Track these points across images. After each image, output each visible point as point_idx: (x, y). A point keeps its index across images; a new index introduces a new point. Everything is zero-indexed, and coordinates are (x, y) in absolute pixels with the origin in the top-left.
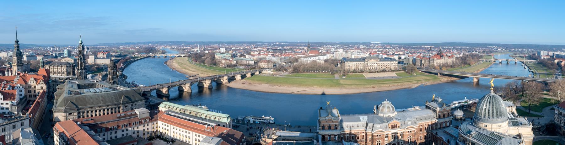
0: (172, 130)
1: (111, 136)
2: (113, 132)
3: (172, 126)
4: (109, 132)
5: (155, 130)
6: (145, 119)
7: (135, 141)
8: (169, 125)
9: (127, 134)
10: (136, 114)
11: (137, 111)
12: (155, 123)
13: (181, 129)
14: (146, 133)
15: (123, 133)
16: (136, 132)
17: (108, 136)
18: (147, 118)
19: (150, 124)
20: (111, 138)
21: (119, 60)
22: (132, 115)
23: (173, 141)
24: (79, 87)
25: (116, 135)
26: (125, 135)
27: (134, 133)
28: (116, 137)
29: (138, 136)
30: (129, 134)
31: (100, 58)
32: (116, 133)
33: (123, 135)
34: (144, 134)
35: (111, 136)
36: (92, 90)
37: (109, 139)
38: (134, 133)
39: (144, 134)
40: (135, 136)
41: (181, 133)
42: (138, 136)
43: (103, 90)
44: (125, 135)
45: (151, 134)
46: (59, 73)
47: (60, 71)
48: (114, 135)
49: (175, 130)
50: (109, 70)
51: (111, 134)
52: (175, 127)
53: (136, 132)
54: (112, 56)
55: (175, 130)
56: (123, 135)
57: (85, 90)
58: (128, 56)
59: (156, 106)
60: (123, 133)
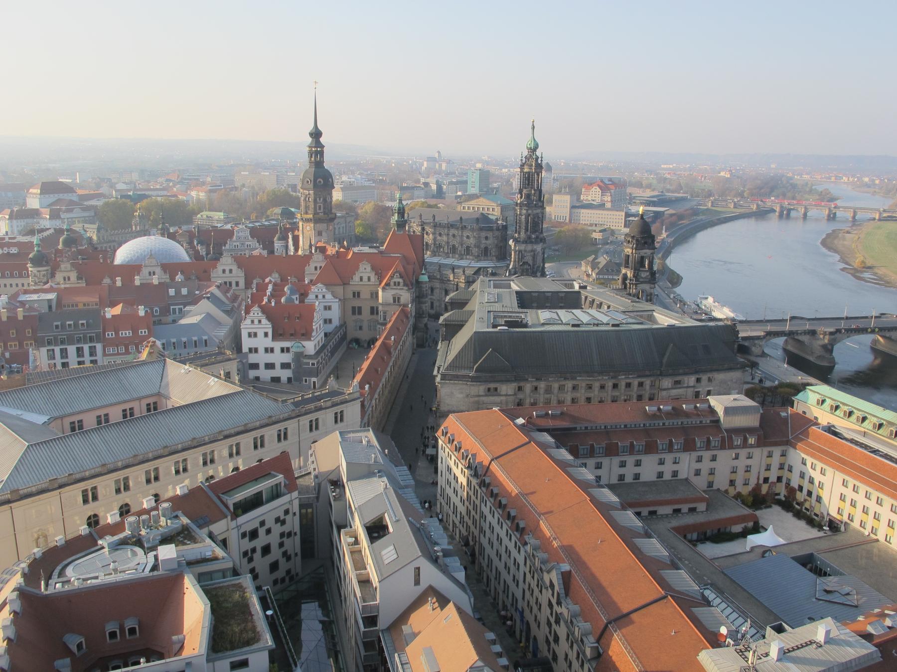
0: (839, 489)
1: (622, 471)
2: (630, 460)
3: (840, 476)
4: (616, 460)
5: (773, 479)
6: (743, 432)
7: (702, 500)
8: (829, 471)
9: (675, 474)
10: (712, 411)
11: (718, 403)
12: (777, 451)
13: (875, 494)
14: (739, 482)
15: (661, 468)
16: (705, 472)
17: (611, 468)
18: (750, 430)
19: (757, 452)
20: (622, 477)
21: (657, 215)
22: (697, 412)
23: (834, 526)
24: (525, 300)
25: (637, 470)
26: (667, 476)
27: (698, 473)
28: (637, 476)
29: (710, 485)
30: (682, 475)
31: (589, 206)
32: (638, 464)
33: (660, 475)
34: (732, 483)
35: (622, 471)
36: (565, 315)
37: (614, 480)
38: (698, 473)
39: (732, 483)
40: (700, 483)
41: (872, 506)
42: (710, 485)
43: (605, 319)
44: (667, 476)
45: (758, 487)
46: (454, 250)
47: (455, 242)
48: (629, 471)
49: (849, 494)
50: (628, 251)
51: (623, 465)
52: (851, 482)
53: (705, 472)
54: (632, 200)
55: (849, 494)
56: (660, 475)
57: (544, 315)
58: (688, 205)
59: (786, 394)
60: (661, 468)
